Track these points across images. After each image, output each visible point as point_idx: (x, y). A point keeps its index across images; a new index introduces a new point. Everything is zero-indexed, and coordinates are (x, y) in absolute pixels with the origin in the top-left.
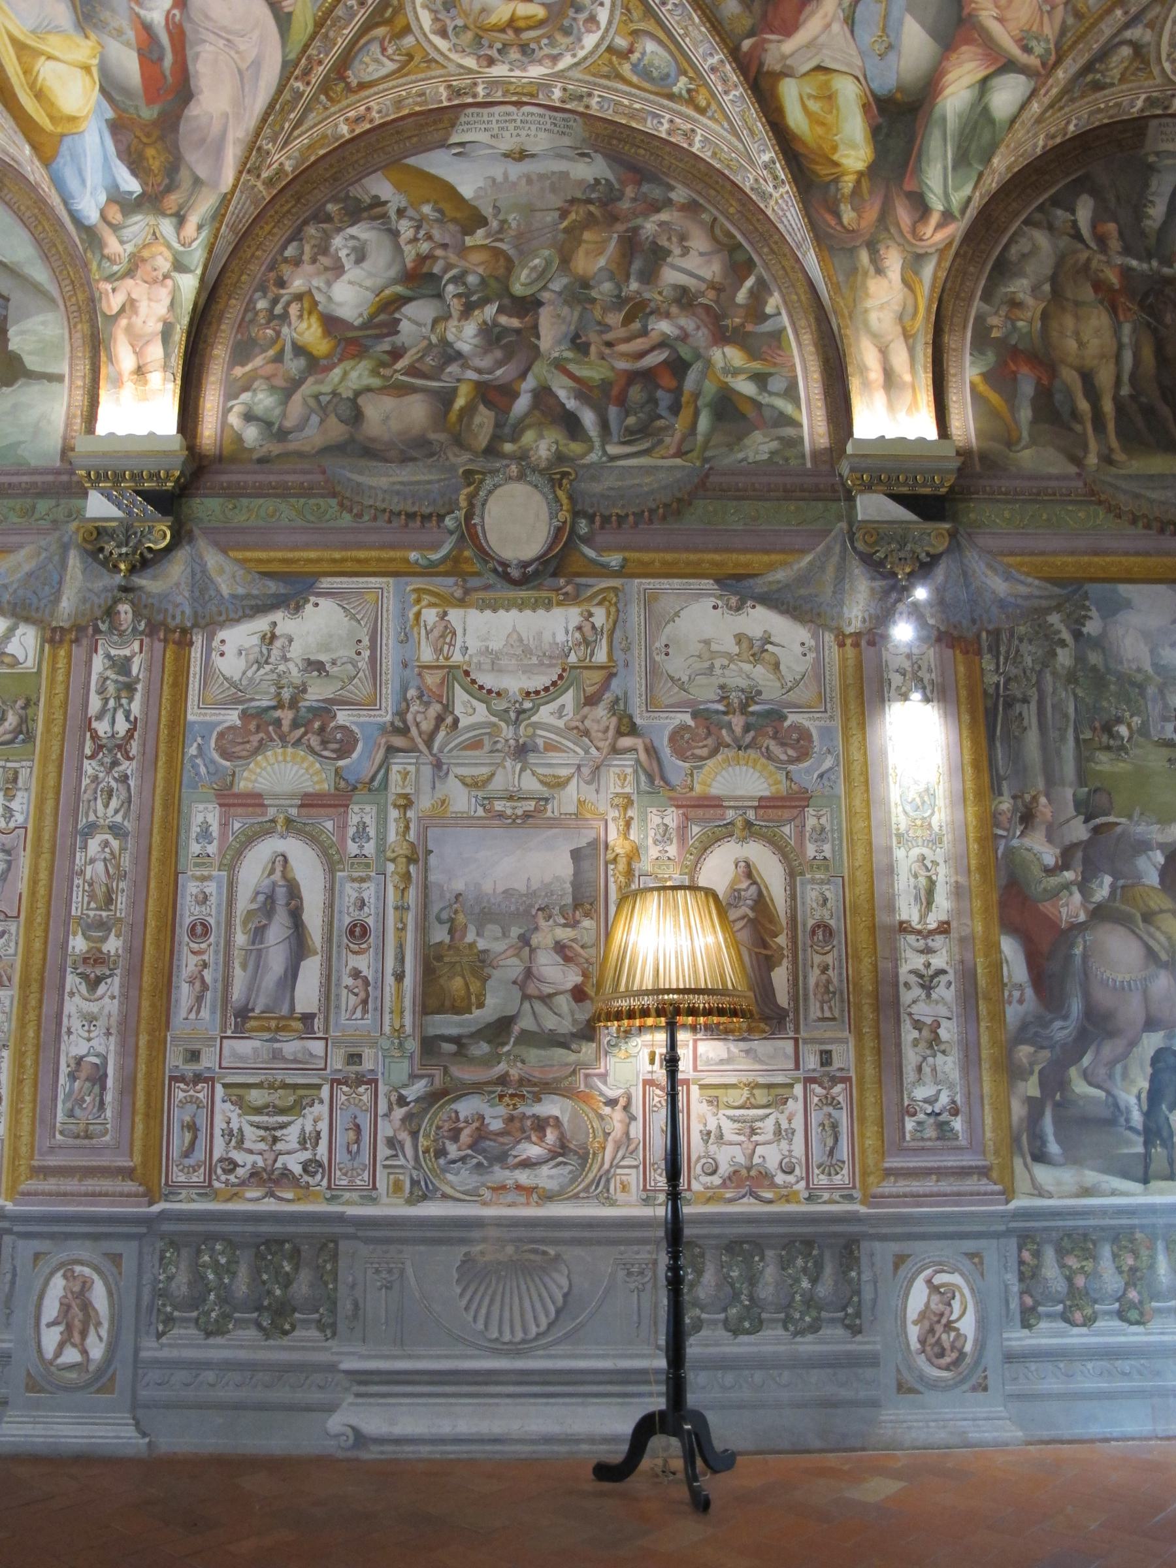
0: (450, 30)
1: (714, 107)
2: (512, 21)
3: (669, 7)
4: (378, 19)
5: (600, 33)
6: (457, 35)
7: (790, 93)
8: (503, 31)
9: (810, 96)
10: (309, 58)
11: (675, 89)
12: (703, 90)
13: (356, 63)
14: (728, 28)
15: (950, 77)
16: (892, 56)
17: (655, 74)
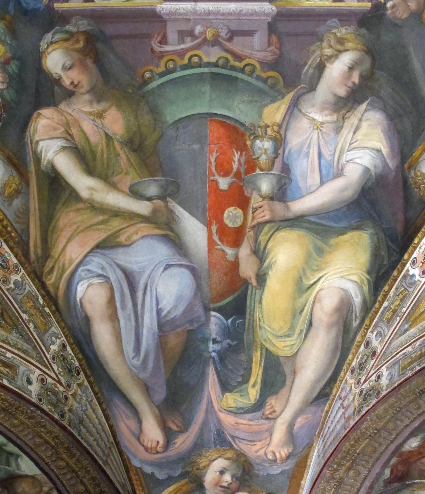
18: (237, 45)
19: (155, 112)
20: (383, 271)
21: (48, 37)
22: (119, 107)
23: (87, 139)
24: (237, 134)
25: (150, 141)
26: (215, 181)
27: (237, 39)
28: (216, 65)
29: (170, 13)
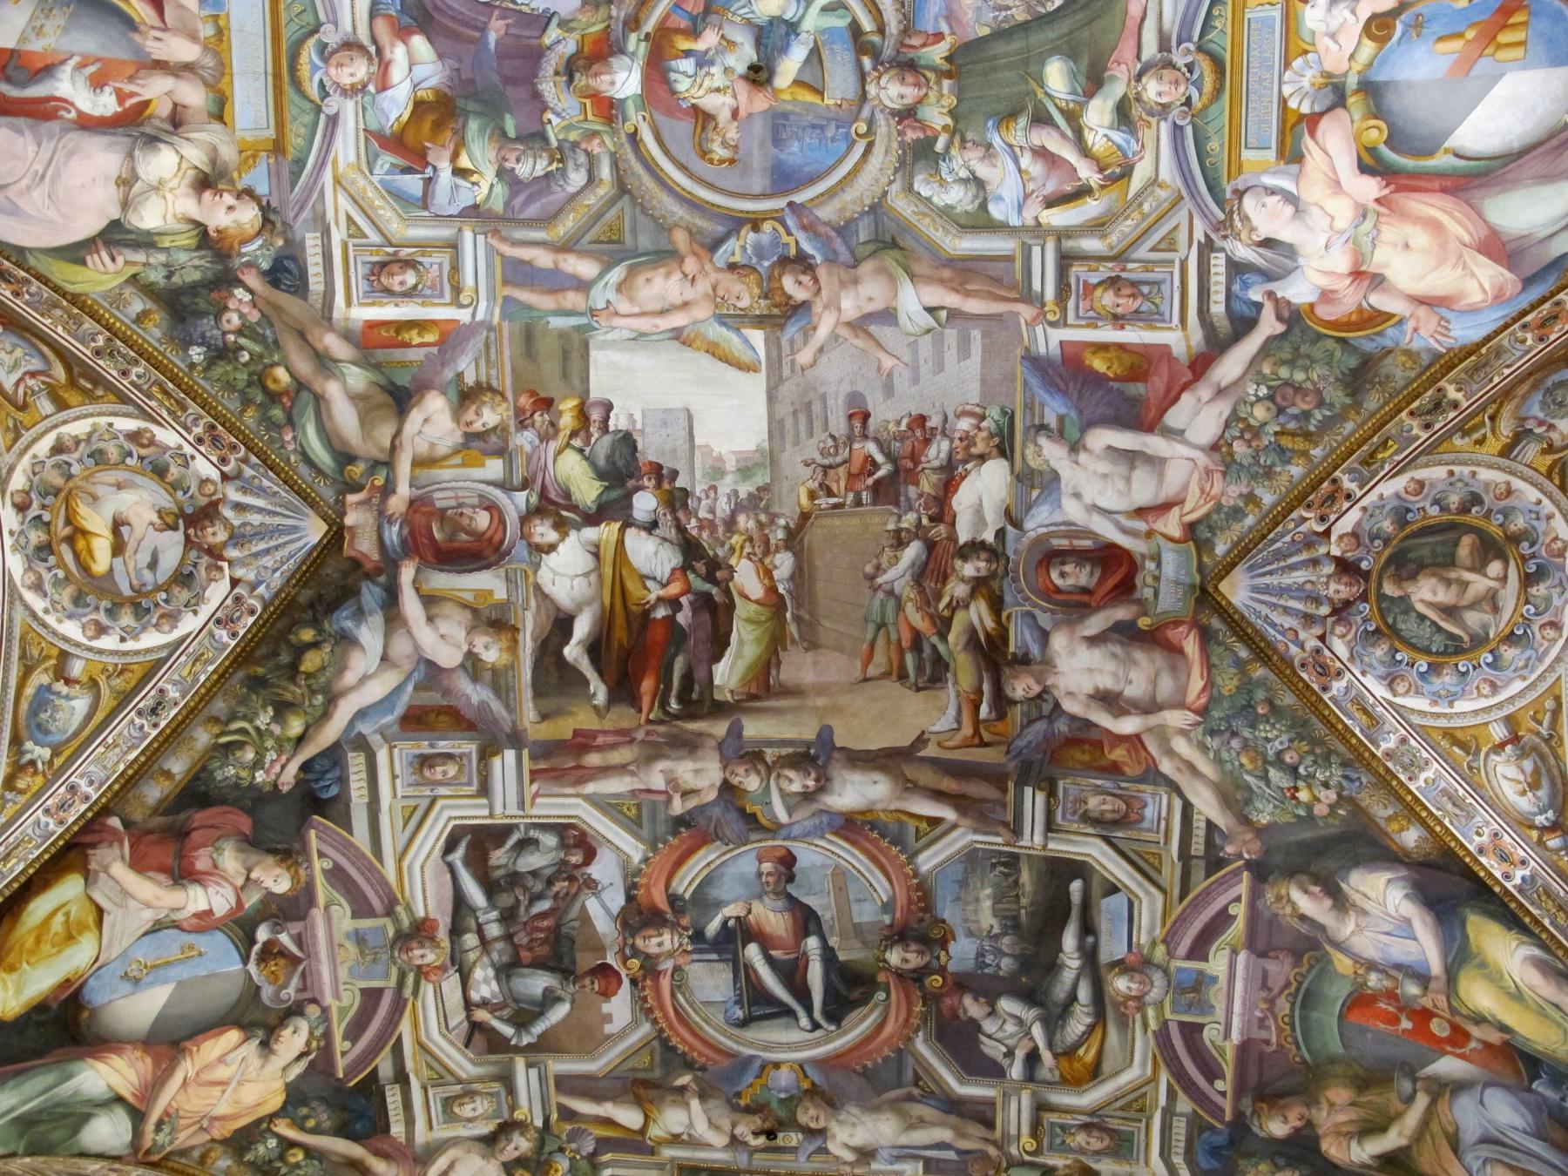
0: (64, 457)
1: (22, 799)
2: (85, 533)
3: (137, 721)
4: (76, 370)
5: (84, 641)
6: (57, 466)
7: (69, 889)
8: (68, 522)
9: (67, 914)
10: (27, 282)
11: (29, 745)
12: (39, 780)
13: (15, 340)
14: (130, 795)
15: (116, 1060)
16: (128, 987)
17: (44, 716)
18: (1276, 983)
19: (1333, 1060)
20: (1510, 916)
21: (1255, 1129)
22: (1326, 1088)
23: (1352, 1122)
24: (1360, 1000)
25: (1360, 1072)
26: (1404, 1031)
27: (1270, 983)
28: (1293, 1004)
29: (1242, 1034)
